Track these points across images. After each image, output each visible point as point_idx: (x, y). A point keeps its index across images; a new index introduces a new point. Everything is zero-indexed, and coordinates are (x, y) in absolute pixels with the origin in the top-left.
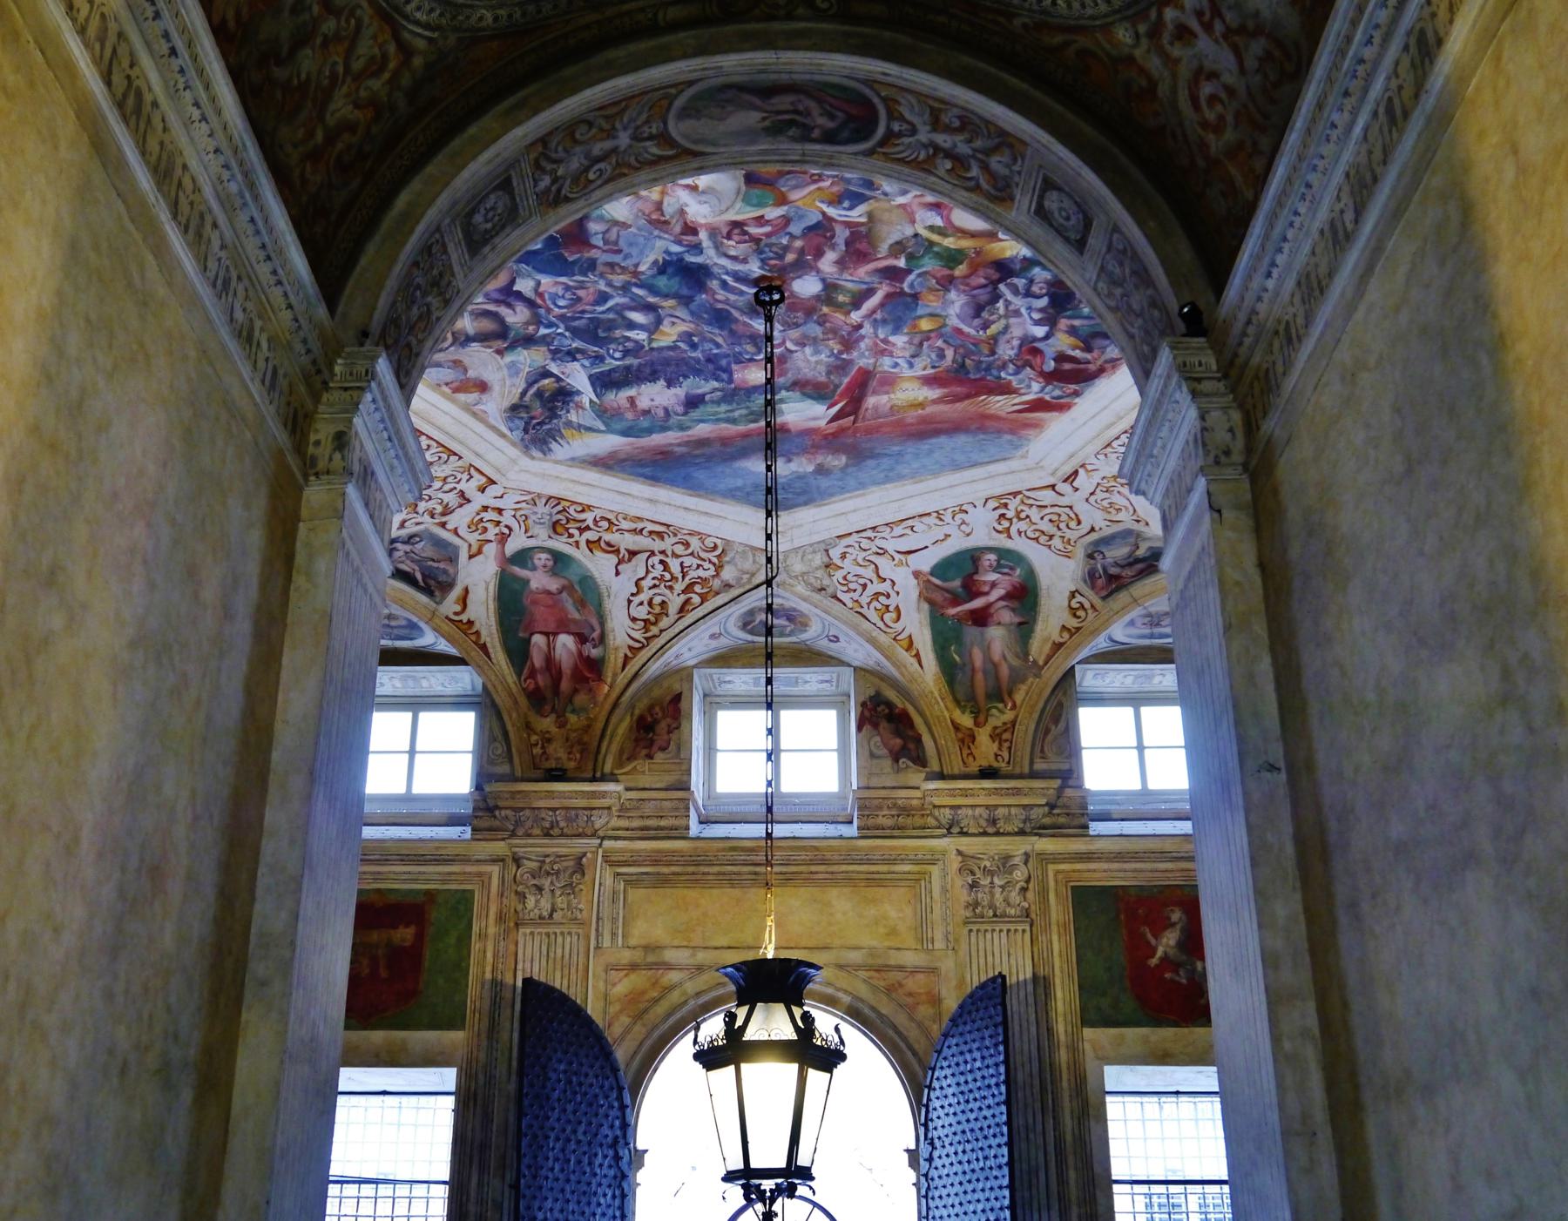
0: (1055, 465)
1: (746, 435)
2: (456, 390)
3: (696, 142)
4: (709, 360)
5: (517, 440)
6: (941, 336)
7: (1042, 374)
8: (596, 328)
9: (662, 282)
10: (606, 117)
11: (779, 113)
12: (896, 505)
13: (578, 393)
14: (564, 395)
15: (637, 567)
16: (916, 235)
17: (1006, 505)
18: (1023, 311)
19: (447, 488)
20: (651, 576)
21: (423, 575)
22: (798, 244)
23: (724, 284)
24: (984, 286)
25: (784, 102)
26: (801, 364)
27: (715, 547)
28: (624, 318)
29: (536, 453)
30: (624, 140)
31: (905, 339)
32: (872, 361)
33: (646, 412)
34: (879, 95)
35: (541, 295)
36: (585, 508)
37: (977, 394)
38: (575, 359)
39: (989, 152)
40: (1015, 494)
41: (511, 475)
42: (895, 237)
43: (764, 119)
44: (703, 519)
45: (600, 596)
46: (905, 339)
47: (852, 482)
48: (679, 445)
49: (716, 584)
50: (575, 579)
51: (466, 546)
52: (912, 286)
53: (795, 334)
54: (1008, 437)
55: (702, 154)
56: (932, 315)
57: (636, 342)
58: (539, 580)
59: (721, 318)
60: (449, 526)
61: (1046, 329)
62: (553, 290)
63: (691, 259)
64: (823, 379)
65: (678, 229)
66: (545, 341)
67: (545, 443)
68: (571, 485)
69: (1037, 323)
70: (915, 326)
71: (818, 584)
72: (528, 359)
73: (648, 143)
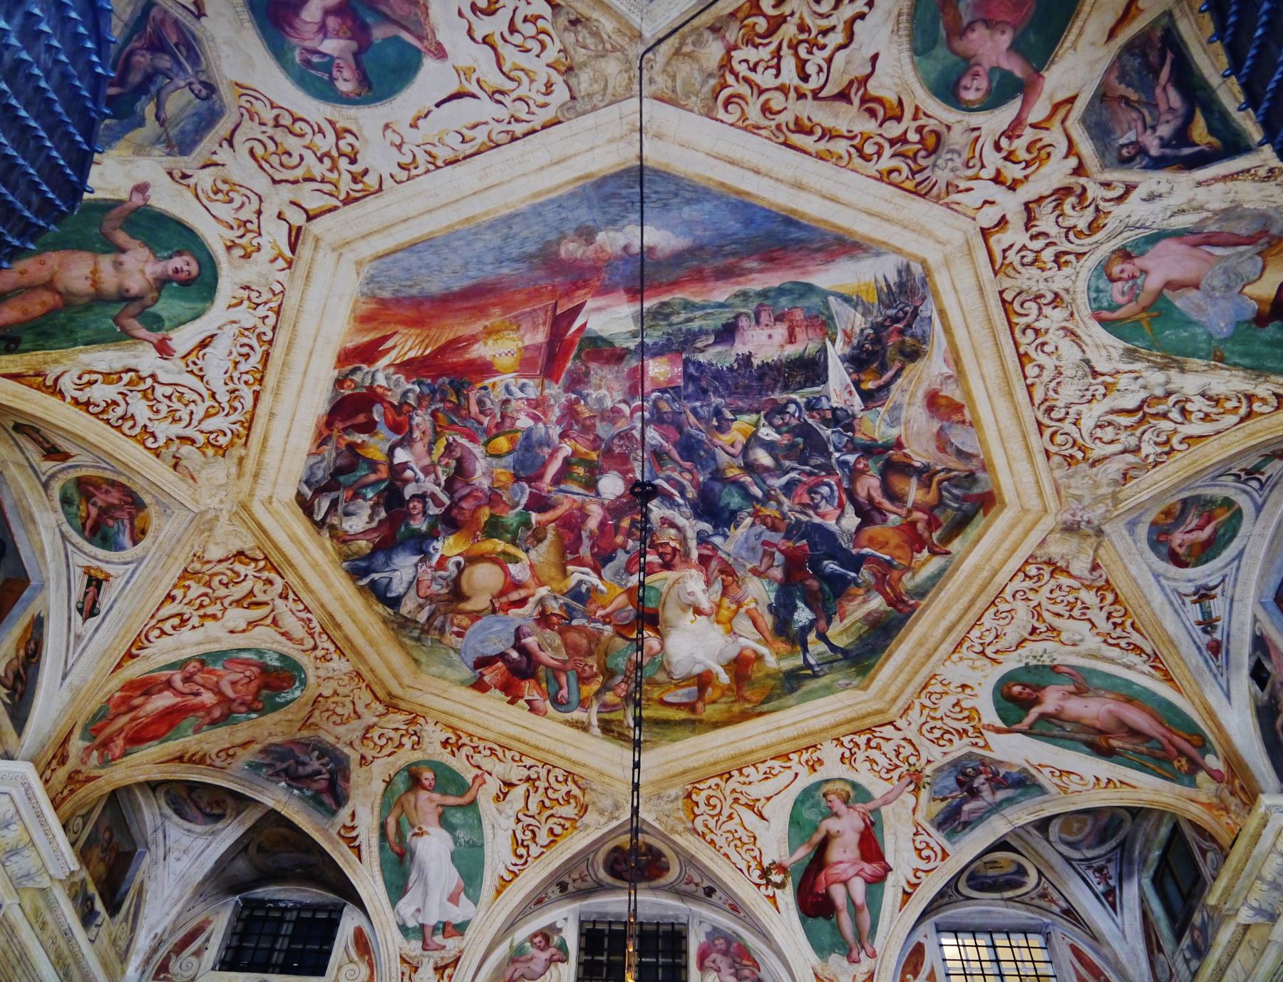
0: (321, 252)
1: (675, 284)
2: (958, 408)
4: (705, 392)
5: (930, 298)
6: (487, 431)
7: (381, 399)
8: (802, 451)
9: (735, 501)
12: (494, 179)
13: (844, 359)
14: (859, 361)
15: (846, 66)
16: (527, 551)
17: (355, 180)
18: (421, 476)
19: (1038, 244)
20: (826, 53)
21: (1157, 76)
22: (619, 539)
23: (683, 495)
24: (463, 498)
26: (616, 385)
27: (726, 104)
28: (776, 459)
29: (917, 269)
31: (519, 424)
32: (547, 391)
33: (779, 319)
35: (841, 506)
36: (885, 177)
37: (434, 354)
38: (834, 410)
40: (348, 201)
41: (958, 238)
42: (543, 547)
44: (737, 154)
45: (913, 15)
46: (519, 424)
47: (551, 216)
48: (751, 271)
49: (733, 34)
50: (941, 51)
51: (1068, 123)
52: (523, 492)
53: (622, 425)
54: (386, 294)
56: (499, 456)
57: (771, 424)
58: (993, 48)
59: (690, 449)
60: (1073, 162)
61: (396, 461)
62: (830, 508)
63: (707, 527)
64: (593, 366)
65: (714, 563)
66: (853, 447)
67: (901, 285)
68: (894, 214)
69: (405, 466)
70: (512, 441)
71: (583, 33)
72: (876, 426)
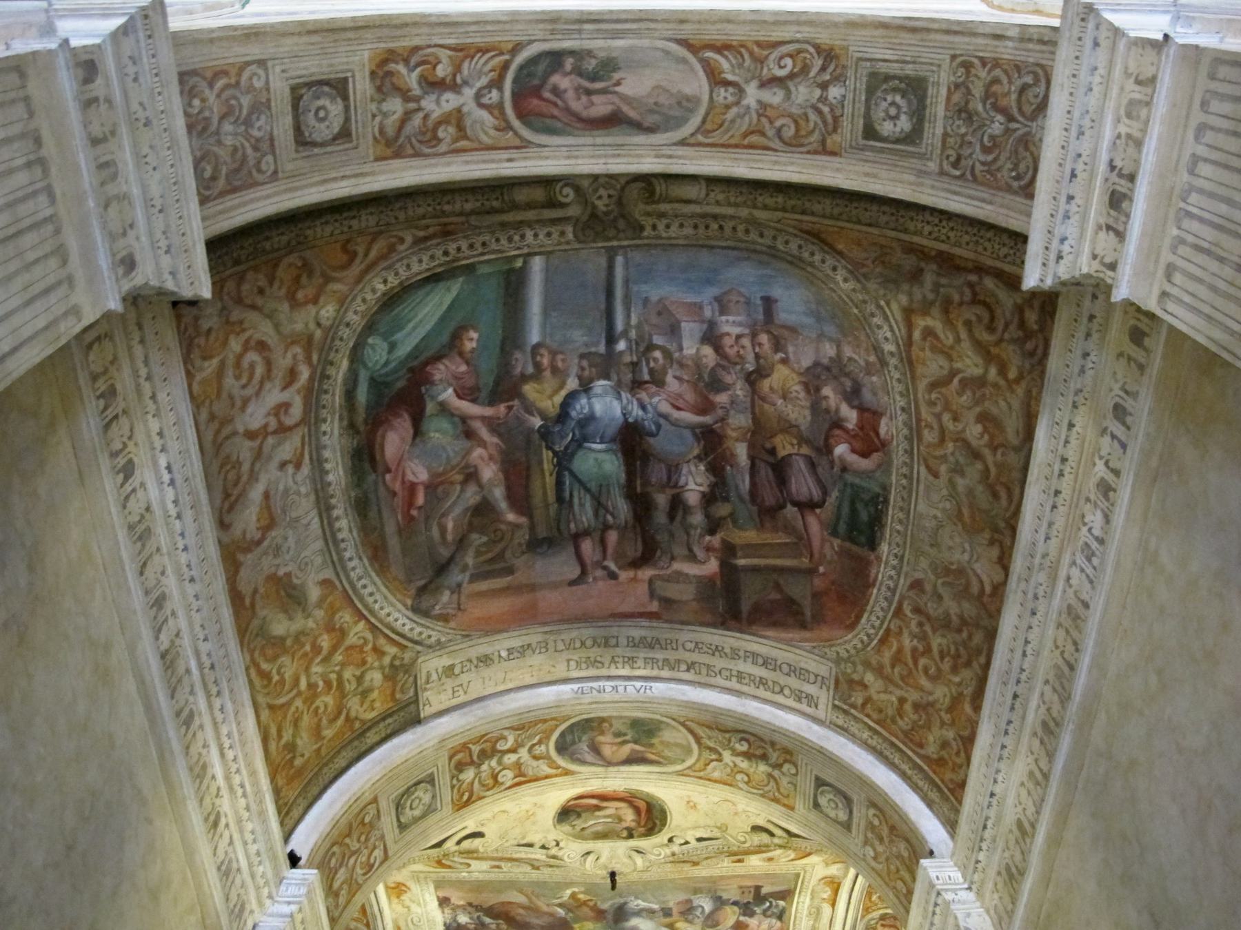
3: (684, 61)
10: (763, 134)
11: (604, 91)
25: (601, 107)
30: (753, 94)
34: (516, 133)
39: (407, 116)
43: (618, 84)
55: (680, 42)
73: (730, 77)
